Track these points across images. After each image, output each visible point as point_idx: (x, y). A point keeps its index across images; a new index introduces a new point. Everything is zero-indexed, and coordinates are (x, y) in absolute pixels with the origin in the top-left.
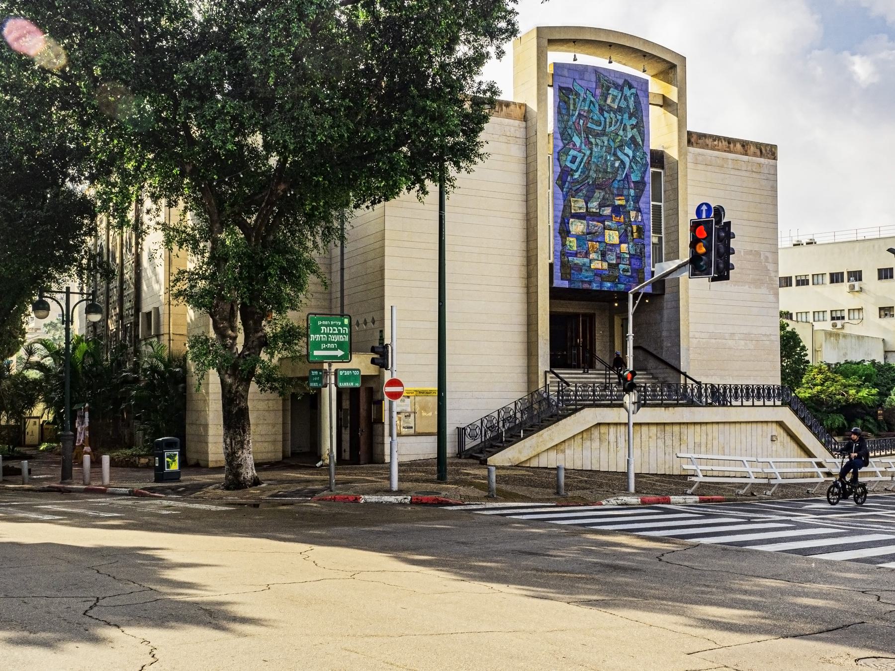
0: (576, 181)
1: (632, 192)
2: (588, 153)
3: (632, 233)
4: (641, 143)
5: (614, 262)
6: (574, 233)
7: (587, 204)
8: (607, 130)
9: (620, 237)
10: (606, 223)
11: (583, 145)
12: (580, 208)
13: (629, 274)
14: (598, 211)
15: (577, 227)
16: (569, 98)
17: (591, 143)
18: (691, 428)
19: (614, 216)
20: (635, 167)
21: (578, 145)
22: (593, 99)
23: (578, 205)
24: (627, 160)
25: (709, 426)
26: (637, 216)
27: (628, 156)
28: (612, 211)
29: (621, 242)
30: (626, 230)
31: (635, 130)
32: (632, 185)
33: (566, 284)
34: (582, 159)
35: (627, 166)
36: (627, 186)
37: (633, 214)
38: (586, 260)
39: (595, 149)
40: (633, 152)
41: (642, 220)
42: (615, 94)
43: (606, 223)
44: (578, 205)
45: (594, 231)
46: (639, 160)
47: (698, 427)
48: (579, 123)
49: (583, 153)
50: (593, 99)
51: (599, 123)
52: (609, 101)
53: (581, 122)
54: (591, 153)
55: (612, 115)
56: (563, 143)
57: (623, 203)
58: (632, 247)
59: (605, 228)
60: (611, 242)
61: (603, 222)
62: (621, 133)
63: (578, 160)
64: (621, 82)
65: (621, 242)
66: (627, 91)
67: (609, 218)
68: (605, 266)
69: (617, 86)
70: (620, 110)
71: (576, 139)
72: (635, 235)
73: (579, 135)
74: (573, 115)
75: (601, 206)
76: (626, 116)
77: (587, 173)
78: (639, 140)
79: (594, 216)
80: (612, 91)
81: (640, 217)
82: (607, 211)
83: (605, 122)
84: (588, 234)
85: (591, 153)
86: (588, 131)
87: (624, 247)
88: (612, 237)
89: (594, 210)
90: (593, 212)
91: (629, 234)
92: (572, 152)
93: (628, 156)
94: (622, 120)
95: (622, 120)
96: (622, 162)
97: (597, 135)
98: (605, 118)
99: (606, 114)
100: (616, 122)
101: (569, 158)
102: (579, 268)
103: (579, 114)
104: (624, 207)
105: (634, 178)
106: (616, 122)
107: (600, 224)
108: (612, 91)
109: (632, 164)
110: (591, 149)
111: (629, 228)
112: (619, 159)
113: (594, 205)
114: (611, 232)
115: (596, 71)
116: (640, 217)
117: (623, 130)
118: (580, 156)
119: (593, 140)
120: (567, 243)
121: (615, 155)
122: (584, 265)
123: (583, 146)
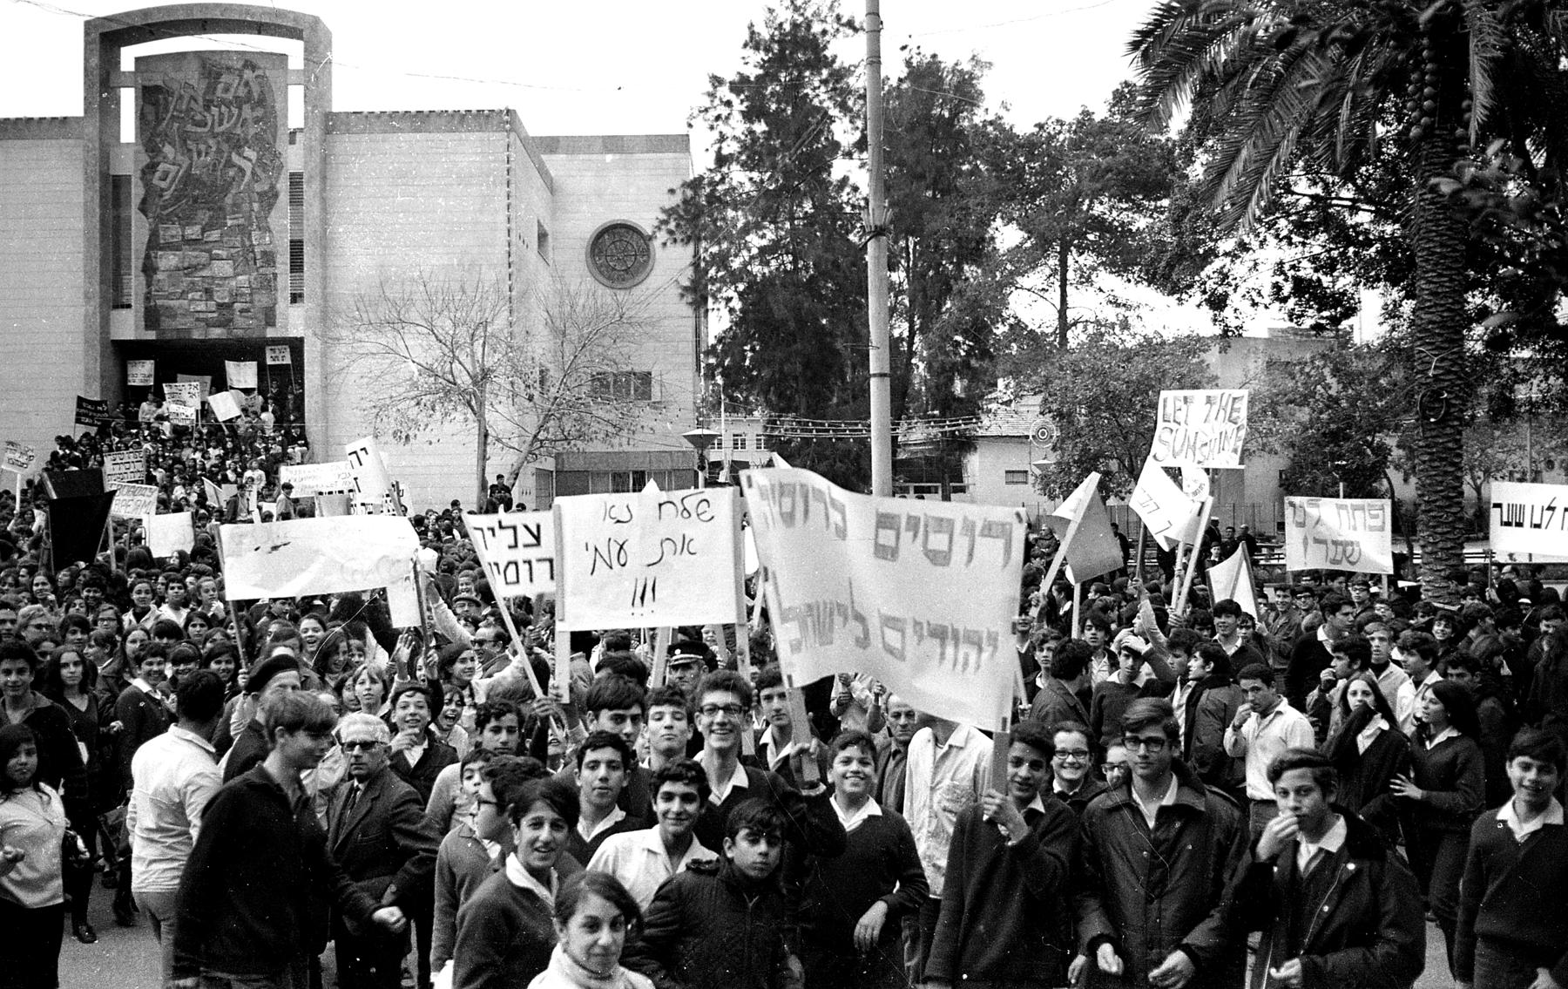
12: (173, 237)
15: (168, 261)
17: (190, 150)
21: (171, 156)
24: (247, 166)
27: (250, 160)
35: (248, 173)
37: (255, 235)
44: (173, 232)
50: (193, 93)
52: (219, 93)
53: (176, 125)
54: (191, 164)
63: (170, 176)
64: (239, 65)
66: (248, 74)
68: (212, 305)
75: (203, 231)
82: (214, 235)
85: (191, 164)
92: (162, 167)
93: (250, 160)
94: (239, 115)
95: (239, 115)
96: (241, 170)
110: (191, 158)
113: (193, 232)
118: (174, 168)
123: (179, 157)
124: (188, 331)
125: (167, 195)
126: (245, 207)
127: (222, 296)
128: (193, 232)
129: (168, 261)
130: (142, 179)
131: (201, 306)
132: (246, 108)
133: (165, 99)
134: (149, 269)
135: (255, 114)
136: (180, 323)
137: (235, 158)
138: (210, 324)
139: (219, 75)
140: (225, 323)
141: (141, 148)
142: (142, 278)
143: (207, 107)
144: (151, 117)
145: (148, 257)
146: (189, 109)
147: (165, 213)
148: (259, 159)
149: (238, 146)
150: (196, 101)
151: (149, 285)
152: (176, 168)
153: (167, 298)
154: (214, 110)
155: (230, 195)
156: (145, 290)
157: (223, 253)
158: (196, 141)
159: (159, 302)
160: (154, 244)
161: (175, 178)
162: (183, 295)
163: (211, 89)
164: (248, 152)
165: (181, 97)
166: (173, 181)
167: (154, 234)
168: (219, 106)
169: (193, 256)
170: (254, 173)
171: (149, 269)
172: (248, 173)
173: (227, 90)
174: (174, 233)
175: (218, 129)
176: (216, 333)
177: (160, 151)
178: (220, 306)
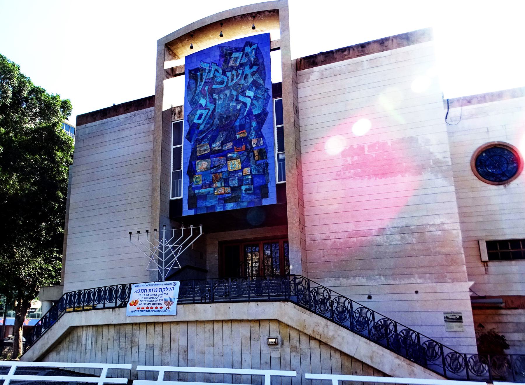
0: (202, 132)
1: (254, 124)
2: (212, 107)
3: (254, 156)
4: (262, 82)
5: (237, 185)
6: (199, 171)
7: (210, 146)
8: (230, 84)
9: (242, 163)
11: (208, 103)
12: (205, 150)
13: (251, 192)
14: (220, 148)
15: (202, 165)
16: (197, 75)
17: (215, 100)
18: (144, 329)
19: (235, 148)
21: (204, 105)
22: (216, 67)
23: (204, 148)
24: (248, 101)
25: (165, 327)
26: (258, 142)
28: (233, 145)
29: (243, 168)
30: (248, 157)
31: (256, 74)
32: (254, 118)
33: (192, 212)
34: (208, 113)
35: (249, 105)
36: (248, 121)
37: (254, 142)
38: (209, 189)
39: (219, 102)
40: (255, 92)
42: (236, 56)
43: (229, 155)
44: (204, 148)
45: (217, 165)
46: (261, 96)
47: (151, 329)
48: (204, 89)
49: (208, 109)
51: (222, 83)
52: (231, 64)
53: (207, 87)
54: (215, 106)
55: (234, 72)
56: (192, 108)
58: (255, 168)
59: (227, 160)
60: (233, 169)
61: (226, 156)
62: (242, 81)
63: (204, 116)
65: (243, 168)
66: (248, 50)
67: (231, 151)
68: (228, 190)
69: (237, 50)
71: (203, 102)
72: (257, 158)
73: (204, 97)
74: (200, 85)
75: (222, 144)
76: (247, 68)
77: (211, 123)
78: (261, 81)
79: (217, 153)
80: (235, 55)
81: (262, 142)
82: (229, 146)
83: (228, 79)
84: (212, 168)
85: (215, 106)
87: (247, 170)
88: (235, 165)
89: (217, 148)
90: (217, 150)
91: (251, 159)
93: (249, 97)
95: (243, 72)
96: (245, 104)
97: (220, 92)
98: (228, 77)
99: (229, 74)
100: (237, 76)
101: (197, 117)
102: (204, 197)
103: (205, 82)
104: (247, 137)
105: (255, 112)
106: (237, 76)
107: (225, 158)
109: (254, 102)
110: (215, 104)
111: (251, 154)
112: (241, 102)
113: (216, 146)
114: (233, 162)
115: (219, 47)
116: (262, 142)
117: (245, 79)
118: (204, 112)
119: (216, 97)
120: (194, 180)
121: (237, 99)
122: (209, 192)
123: (208, 104)
124: (214, 207)
125: (202, 127)
126: (247, 126)
127: (234, 183)
128: (216, 146)
129: (202, 165)
130: (188, 121)
131: (222, 191)
133: (201, 75)
134: (191, 171)
135: (252, 70)
136: (209, 203)
137: (241, 98)
139: (231, 54)
142: (187, 177)
144: (193, 86)
145: (190, 163)
146: (214, 76)
147: (201, 137)
149: (243, 93)
150: (218, 72)
151: (191, 182)
152: (207, 111)
153: (201, 188)
154: (229, 74)
155: (238, 121)
156: (188, 185)
157: (234, 155)
159: (196, 191)
160: (194, 157)
161: (206, 117)
162: (210, 185)
163: (227, 61)
164: (250, 93)
165: (210, 71)
166: (204, 119)
167: (194, 151)
168: (231, 71)
169: (218, 160)
170: (252, 104)
171: (191, 171)
172: (249, 105)
174: (205, 148)
175: (230, 84)
176: (230, 206)
177: (198, 102)
178: (233, 189)
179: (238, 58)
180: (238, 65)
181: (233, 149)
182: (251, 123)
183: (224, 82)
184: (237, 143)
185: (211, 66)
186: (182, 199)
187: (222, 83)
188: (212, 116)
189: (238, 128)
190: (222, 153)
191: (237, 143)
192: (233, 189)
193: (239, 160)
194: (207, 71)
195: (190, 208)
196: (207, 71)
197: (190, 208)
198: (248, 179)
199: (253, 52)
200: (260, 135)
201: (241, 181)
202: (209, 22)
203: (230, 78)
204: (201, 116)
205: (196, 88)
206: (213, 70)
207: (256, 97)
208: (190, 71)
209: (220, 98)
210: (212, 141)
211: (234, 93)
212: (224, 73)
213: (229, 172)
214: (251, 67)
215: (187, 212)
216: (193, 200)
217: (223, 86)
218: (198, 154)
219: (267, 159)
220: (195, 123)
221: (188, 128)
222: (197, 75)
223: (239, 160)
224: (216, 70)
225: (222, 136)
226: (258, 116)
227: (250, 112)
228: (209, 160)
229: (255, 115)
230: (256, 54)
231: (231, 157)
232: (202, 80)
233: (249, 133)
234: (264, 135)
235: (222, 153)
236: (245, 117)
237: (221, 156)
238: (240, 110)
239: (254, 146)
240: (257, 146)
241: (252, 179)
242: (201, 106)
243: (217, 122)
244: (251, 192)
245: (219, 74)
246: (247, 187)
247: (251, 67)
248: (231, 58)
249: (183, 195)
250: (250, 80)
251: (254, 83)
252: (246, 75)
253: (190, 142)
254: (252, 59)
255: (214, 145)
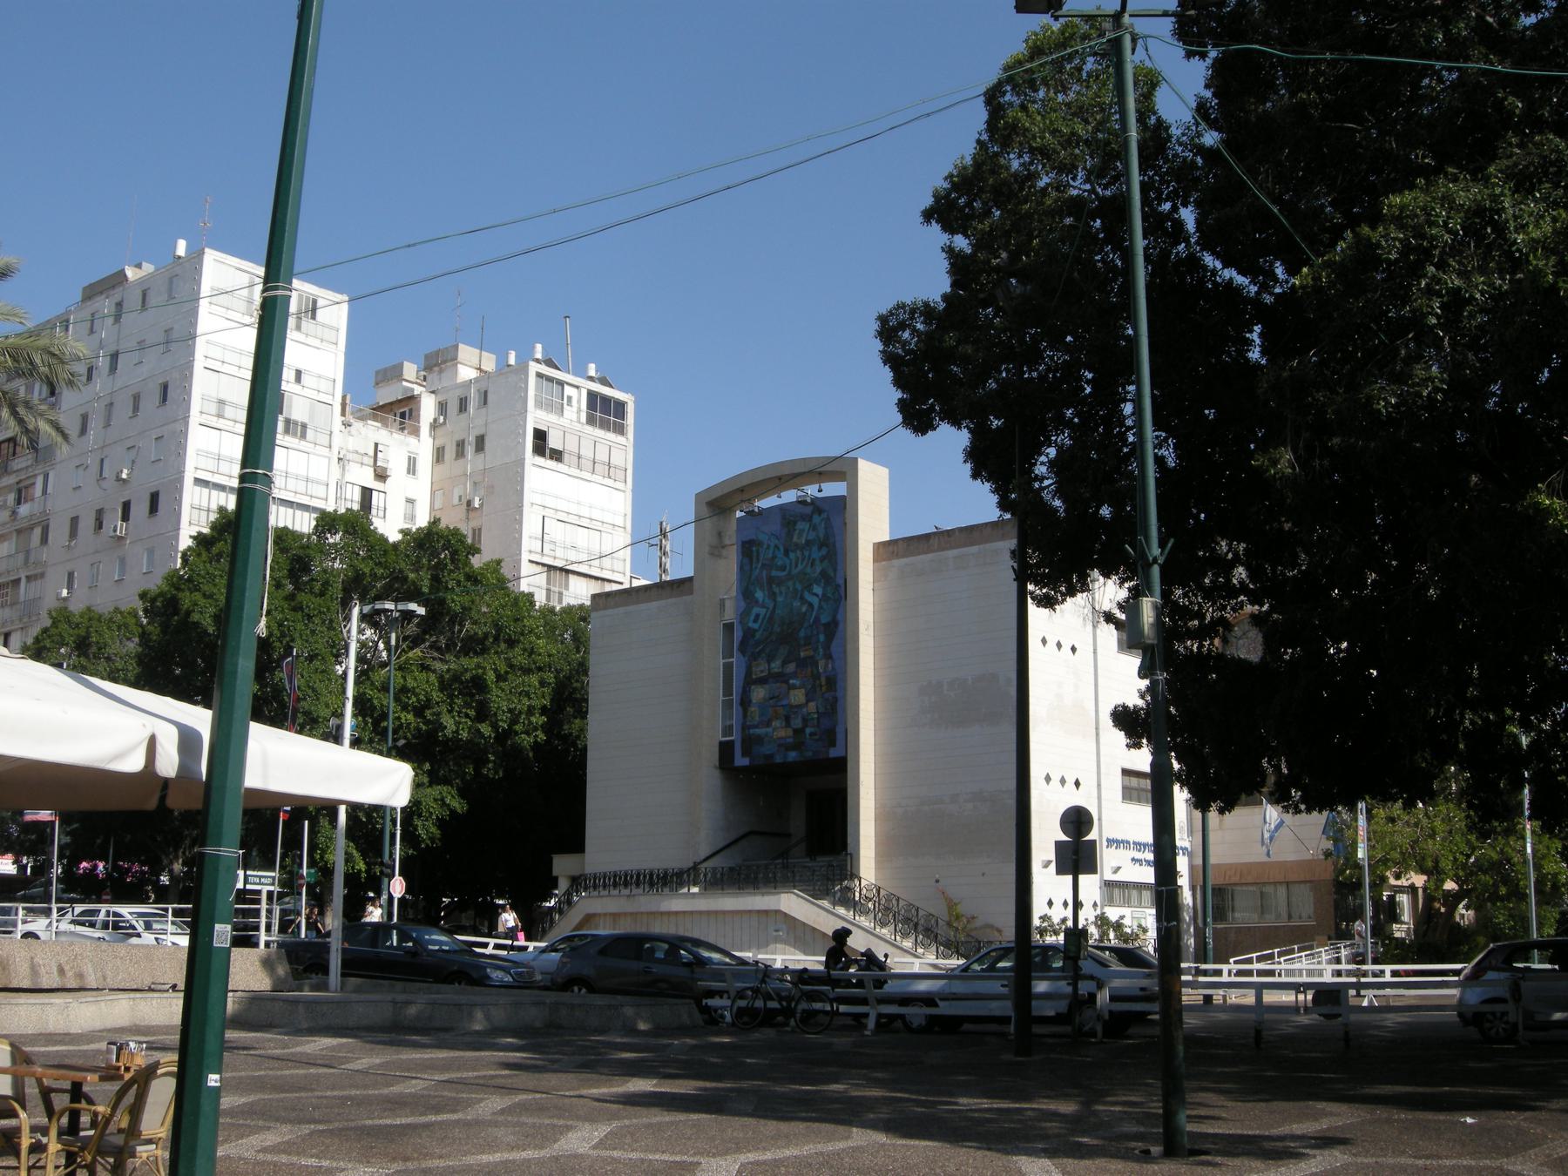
1: (822, 637)
5: (800, 726)
7: (769, 665)
9: (807, 695)
10: (791, 681)
12: (762, 671)
13: (817, 737)
15: (759, 693)
17: (774, 594)
20: (825, 607)
21: (761, 600)
23: (761, 668)
24: (815, 601)
26: (826, 665)
27: (817, 595)
28: (797, 666)
29: (808, 701)
31: (826, 561)
35: (816, 606)
37: (821, 664)
39: (780, 599)
40: (824, 588)
41: (833, 668)
42: (801, 527)
43: (791, 681)
44: (761, 668)
51: (783, 568)
52: (795, 539)
53: (764, 573)
55: (799, 553)
57: (811, 653)
63: (761, 617)
65: (808, 701)
66: (816, 519)
67: (794, 675)
68: (790, 732)
69: (804, 518)
70: (808, 543)
71: (759, 595)
73: (762, 588)
75: (784, 663)
76: (815, 548)
80: (801, 525)
82: (791, 667)
84: (771, 699)
86: (771, 580)
87: (812, 705)
88: (797, 697)
89: (776, 670)
91: (818, 689)
93: (817, 595)
94: (810, 556)
95: (810, 556)
96: (811, 605)
100: (803, 559)
101: (752, 617)
102: (759, 740)
103: (763, 565)
104: (811, 657)
105: (824, 619)
106: (803, 559)
107: (784, 685)
108: (801, 525)
110: (775, 600)
112: (807, 601)
113: (776, 666)
117: (812, 565)
118: (762, 611)
119: (776, 590)
121: (802, 598)
122: (766, 735)
123: (767, 601)
124: (771, 756)
125: (758, 635)
127: (797, 723)
128: (776, 666)
129: (759, 693)
131: (782, 733)
132: (815, 548)
134: (745, 702)
135: (820, 554)
136: (766, 749)
138: (788, 748)
139: (795, 523)
140: (798, 746)
141: (741, 596)
142: (740, 708)
143: (786, 553)
144: (747, 568)
145: (744, 688)
146: (774, 557)
148: (824, 595)
149: (809, 588)
151: (745, 715)
152: (765, 610)
154: (792, 555)
158: (779, 585)
159: (751, 731)
161: (764, 619)
162: (768, 724)
163: (790, 534)
164: (818, 590)
165: (769, 546)
167: (749, 673)
170: (820, 607)
172: (816, 606)
173: (800, 535)
174: (762, 668)
175: (795, 572)
176: (792, 756)
178: (796, 731)
179: (804, 530)
180: (803, 542)
181: (795, 673)
182: (818, 634)
183: (785, 567)
184: (802, 663)
185: (769, 539)
186: (732, 741)
187: (783, 568)
188: (771, 618)
189: (802, 642)
190: (781, 677)
191: (802, 663)
192: (796, 731)
193: (803, 691)
194: (765, 546)
195: (744, 755)
196: (765, 546)
197: (744, 755)
198: (813, 719)
199: (823, 525)
200: (829, 656)
201: (805, 721)
202: (761, 478)
203: (794, 561)
204: (757, 616)
205: (751, 570)
206: (772, 545)
207: (825, 598)
208: (744, 543)
209: (781, 593)
210: (770, 660)
211: (799, 587)
212: (786, 553)
213: (791, 706)
214: (820, 549)
215: (741, 761)
216: (749, 743)
217: (784, 573)
218: (754, 677)
219: (836, 691)
220: (749, 628)
221: (741, 634)
222: (752, 551)
223: (803, 691)
224: (776, 546)
225: (783, 651)
226: (827, 625)
227: (817, 619)
228: (767, 686)
229: (824, 624)
230: (826, 528)
231: (793, 684)
232: (758, 560)
233: (815, 650)
234: (834, 656)
235: (781, 677)
236: (811, 626)
237: (782, 682)
238: (805, 613)
239: (821, 671)
240: (825, 672)
241: (818, 718)
242: (757, 602)
243: (777, 629)
244: (817, 737)
245: (780, 554)
246: (813, 730)
247: (820, 549)
248: (795, 530)
249: (735, 737)
250: (818, 569)
251: (823, 574)
252: (814, 560)
253: (744, 656)
254: (821, 535)
255: (773, 665)
